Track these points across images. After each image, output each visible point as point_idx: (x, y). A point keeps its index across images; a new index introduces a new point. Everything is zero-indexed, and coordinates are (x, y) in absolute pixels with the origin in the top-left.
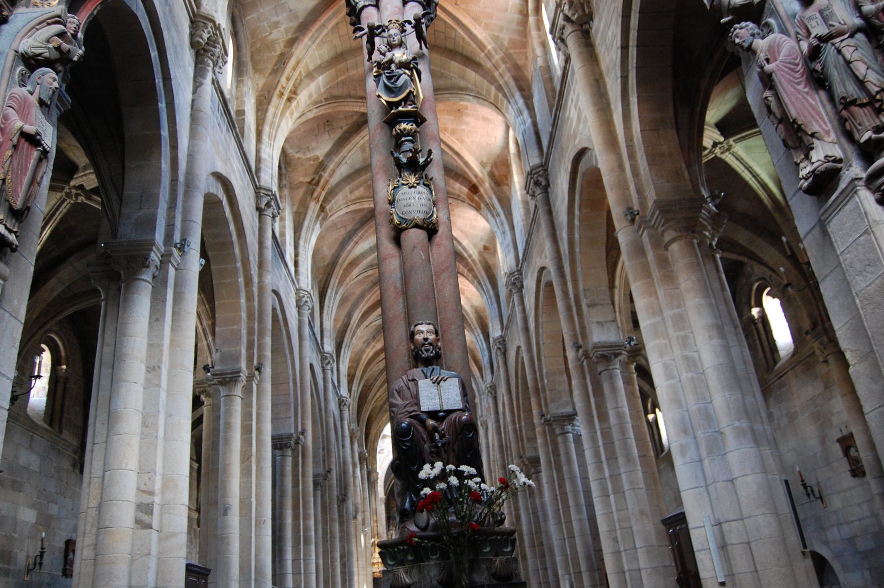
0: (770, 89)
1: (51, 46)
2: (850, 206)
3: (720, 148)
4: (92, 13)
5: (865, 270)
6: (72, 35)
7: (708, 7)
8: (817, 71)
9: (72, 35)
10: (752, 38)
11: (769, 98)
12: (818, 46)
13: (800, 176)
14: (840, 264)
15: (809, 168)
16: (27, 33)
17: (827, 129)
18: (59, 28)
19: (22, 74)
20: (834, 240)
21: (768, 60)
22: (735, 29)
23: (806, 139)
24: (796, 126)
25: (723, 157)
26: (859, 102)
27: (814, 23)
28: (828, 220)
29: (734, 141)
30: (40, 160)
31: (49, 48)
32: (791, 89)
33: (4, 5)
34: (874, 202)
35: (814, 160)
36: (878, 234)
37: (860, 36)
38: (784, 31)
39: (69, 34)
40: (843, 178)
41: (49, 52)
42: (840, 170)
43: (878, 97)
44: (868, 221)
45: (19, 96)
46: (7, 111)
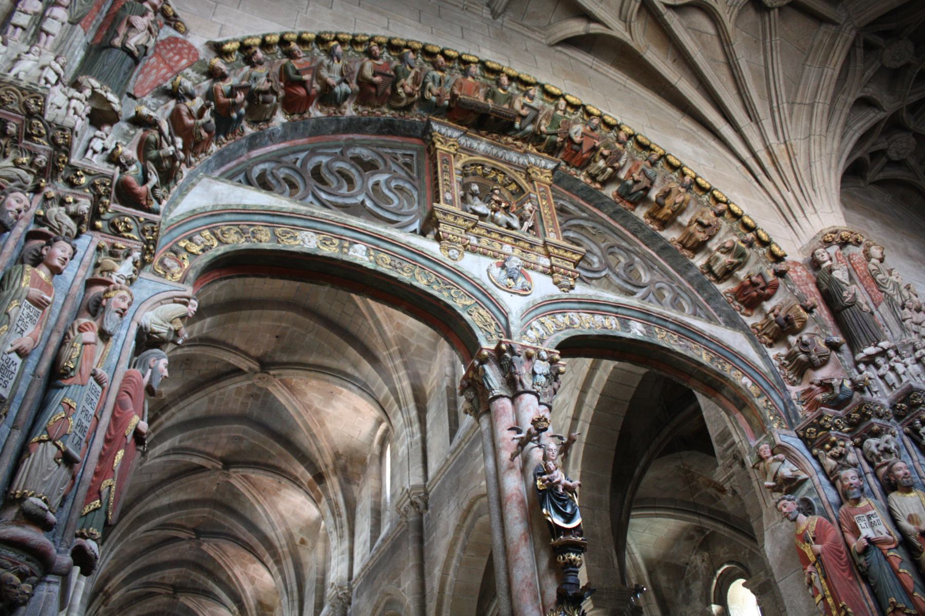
21: (814, 539)
27: (863, 524)
31: (170, 330)
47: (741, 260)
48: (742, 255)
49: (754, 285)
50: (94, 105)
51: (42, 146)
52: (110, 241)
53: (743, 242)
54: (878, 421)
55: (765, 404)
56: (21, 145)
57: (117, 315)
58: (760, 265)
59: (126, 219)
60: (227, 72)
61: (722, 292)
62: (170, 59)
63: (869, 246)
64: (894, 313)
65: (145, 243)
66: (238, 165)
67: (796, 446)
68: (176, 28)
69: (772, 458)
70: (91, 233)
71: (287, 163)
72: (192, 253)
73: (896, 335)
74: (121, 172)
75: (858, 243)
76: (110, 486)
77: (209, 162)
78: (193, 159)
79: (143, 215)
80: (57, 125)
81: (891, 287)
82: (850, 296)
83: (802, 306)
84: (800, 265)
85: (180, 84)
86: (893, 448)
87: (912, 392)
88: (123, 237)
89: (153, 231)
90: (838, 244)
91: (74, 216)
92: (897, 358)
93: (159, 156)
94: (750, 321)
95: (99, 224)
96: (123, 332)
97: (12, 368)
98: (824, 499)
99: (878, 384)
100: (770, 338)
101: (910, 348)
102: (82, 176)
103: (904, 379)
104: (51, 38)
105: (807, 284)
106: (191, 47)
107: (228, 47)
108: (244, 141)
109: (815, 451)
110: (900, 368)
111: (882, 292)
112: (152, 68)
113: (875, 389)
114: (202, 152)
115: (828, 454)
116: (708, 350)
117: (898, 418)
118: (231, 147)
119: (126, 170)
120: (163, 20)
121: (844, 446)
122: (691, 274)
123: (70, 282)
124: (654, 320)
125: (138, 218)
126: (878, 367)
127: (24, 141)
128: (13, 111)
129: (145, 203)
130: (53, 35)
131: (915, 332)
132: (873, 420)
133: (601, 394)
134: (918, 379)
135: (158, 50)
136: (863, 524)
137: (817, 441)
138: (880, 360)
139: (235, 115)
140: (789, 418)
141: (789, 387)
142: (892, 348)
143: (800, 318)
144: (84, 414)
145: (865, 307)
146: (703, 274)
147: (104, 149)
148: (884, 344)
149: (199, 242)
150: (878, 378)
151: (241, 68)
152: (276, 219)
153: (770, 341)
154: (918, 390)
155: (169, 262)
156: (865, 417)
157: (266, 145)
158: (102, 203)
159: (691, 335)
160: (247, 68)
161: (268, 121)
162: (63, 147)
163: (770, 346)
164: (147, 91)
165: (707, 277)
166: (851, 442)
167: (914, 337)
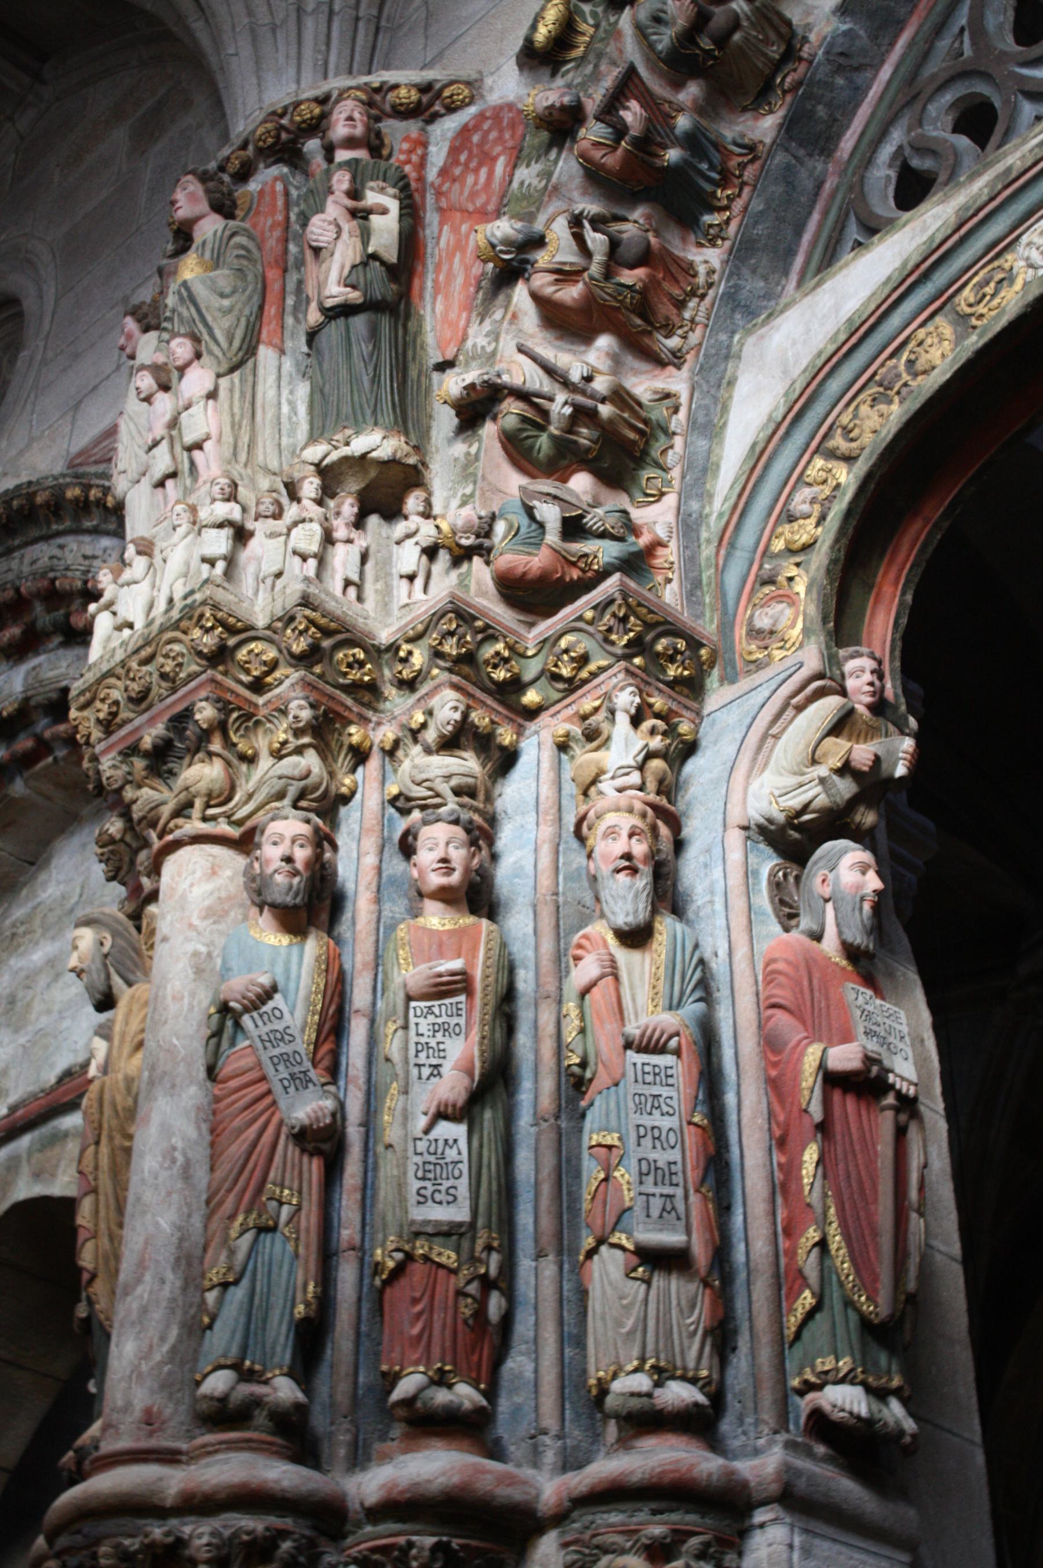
1: (823, 771)
4: (901, 603)
6: (870, 707)
9: (870, 707)
16: (754, 760)
18: (829, 706)
19: (778, 885)
30: (901, 1133)
31: (822, 781)
33: (674, 707)
39: (861, 709)
41: (826, 791)
45: (788, 962)
46: (771, 1024)
50: (354, 485)
51: (287, 683)
52: (570, 711)
56: (263, 712)
57: (622, 877)
59: (563, 643)
60: (566, 100)
62: (473, 195)
65: (628, 657)
66: (825, 213)
68: (451, 109)
70: (532, 726)
71: (933, 77)
72: (807, 548)
74: (488, 563)
76: (822, 1244)
77: (731, 298)
78: (674, 342)
79: (583, 605)
80: (279, 619)
85: (493, 246)
88: (585, 682)
89: (624, 620)
91: (449, 744)
93: (552, 437)
95: (531, 697)
96: (717, 873)
97: (451, 1154)
102: (410, 653)
104: (208, 446)
106: (497, 113)
107: (542, 34)
108: (780, 158)
112: (451, 257)
114: (680, 305)
118: (757, 205)
119: (489, 550)
120: (412, 127)
123: (531, 872)
125: (580, 618)
127: (261, 701)
128: (192, 677)
129: (575, 574)
130: (208, 438)
135: (444, 204)
139: (673, 155)
144: (647, 1142)
147: (431, 552)
149: (805, 508)
151: (615, 33)
152: (940, 278)
155: (763, 621)
157: (858, 93)
158: (487, 662)
160: (625, 20)
161: (790, 54)
162: (326, 643)
164: (462, 323)
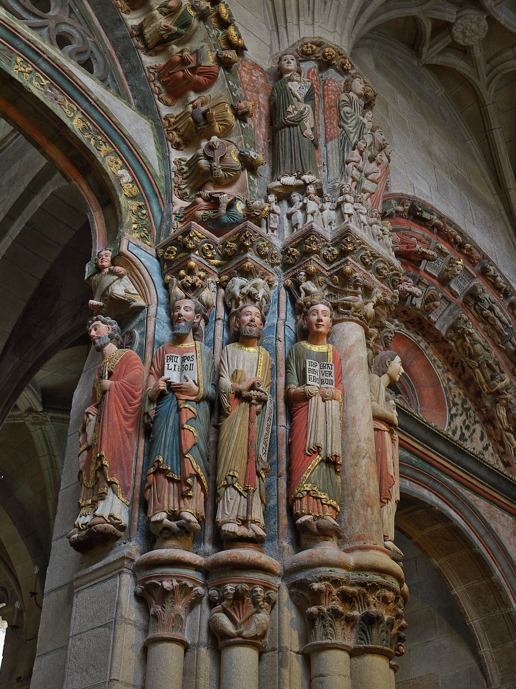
0: (97, 407)
2: (108, 585)
3: (33, 417)
5: (86, 670)
7: (86, 278)
8: (149, 417)
10: (109, 339)
11: (90, 416)
12: (163, 391)
13: (76, 523)
14: (65, 647)
15: (88, 519)
17: (128, 485)
20: (73, 614)
21: (110, 374)
22: (97, 320)
23: (102, 483)
24: (99, 464)
25: (31, 428)
26: (170, 475)
27: (172, 365)
28: (79, 589)
29: (51, 418)
32: (116, 419)
34: (133, 594)
35: (97, 513)
36: (119, 632)
37: (205, 406)
38: (142, 353)
40: (116, 549)
42: (118, 538)
43: (189, 481)
44: (116, 614)
47: (183, 31)
48: (185, 24)
49: (184, 62)
53: (193, 8)
54: (257, 259)
55: (134, 208)
58: (204, 44)
61: (146, 65)
63: (354, 77)
64: (342, 152)
67: (147, 264)
69: (107, 270)
73: (331, 177)
75: (344, 71)
81: (354, 123)
82: (296, 112)
83: (232, 106)
84: (262, 70)
86: (260, 296)
87: (309, 236)
90: (317, 60)
92: (317, 198)
94: (165, 111)
98: (150, 333)
99: (281, 222)
100: (180, 136)
101: (338, 192)
103: (310, 218)
105: (258, 92)
109: (169, 277)
110: (312, 206)
111: (340, 127)
113: (274, 225)
115: (179, 282)
116: (86, 116)
117: (286, 266)
121: (203, 279)
122: (118, 33)
124: (21, 46)
126: (291, 204)
131: (354, 180)
132: (249, 255)
133: (27, 224)
134: (328, 228)
136: (172, 365)
137: (174, 265)
138: (296, 197)
140: (159, 235)
141: (175, 199)
142: (316, 185)
143: (224, 120)
145: (309, 132)
146: (132, 36)
148: (307, 178)
150: (285, 217)
153: (178, 139)
154: (318, 235)
156: (243, 248)
159: (70, 89)
163: (177, 147)
165: (136, 42)
166: (217, 279)
167: (349, 184)
